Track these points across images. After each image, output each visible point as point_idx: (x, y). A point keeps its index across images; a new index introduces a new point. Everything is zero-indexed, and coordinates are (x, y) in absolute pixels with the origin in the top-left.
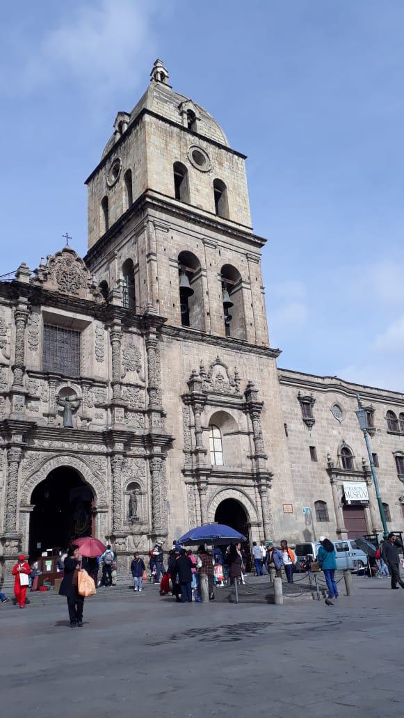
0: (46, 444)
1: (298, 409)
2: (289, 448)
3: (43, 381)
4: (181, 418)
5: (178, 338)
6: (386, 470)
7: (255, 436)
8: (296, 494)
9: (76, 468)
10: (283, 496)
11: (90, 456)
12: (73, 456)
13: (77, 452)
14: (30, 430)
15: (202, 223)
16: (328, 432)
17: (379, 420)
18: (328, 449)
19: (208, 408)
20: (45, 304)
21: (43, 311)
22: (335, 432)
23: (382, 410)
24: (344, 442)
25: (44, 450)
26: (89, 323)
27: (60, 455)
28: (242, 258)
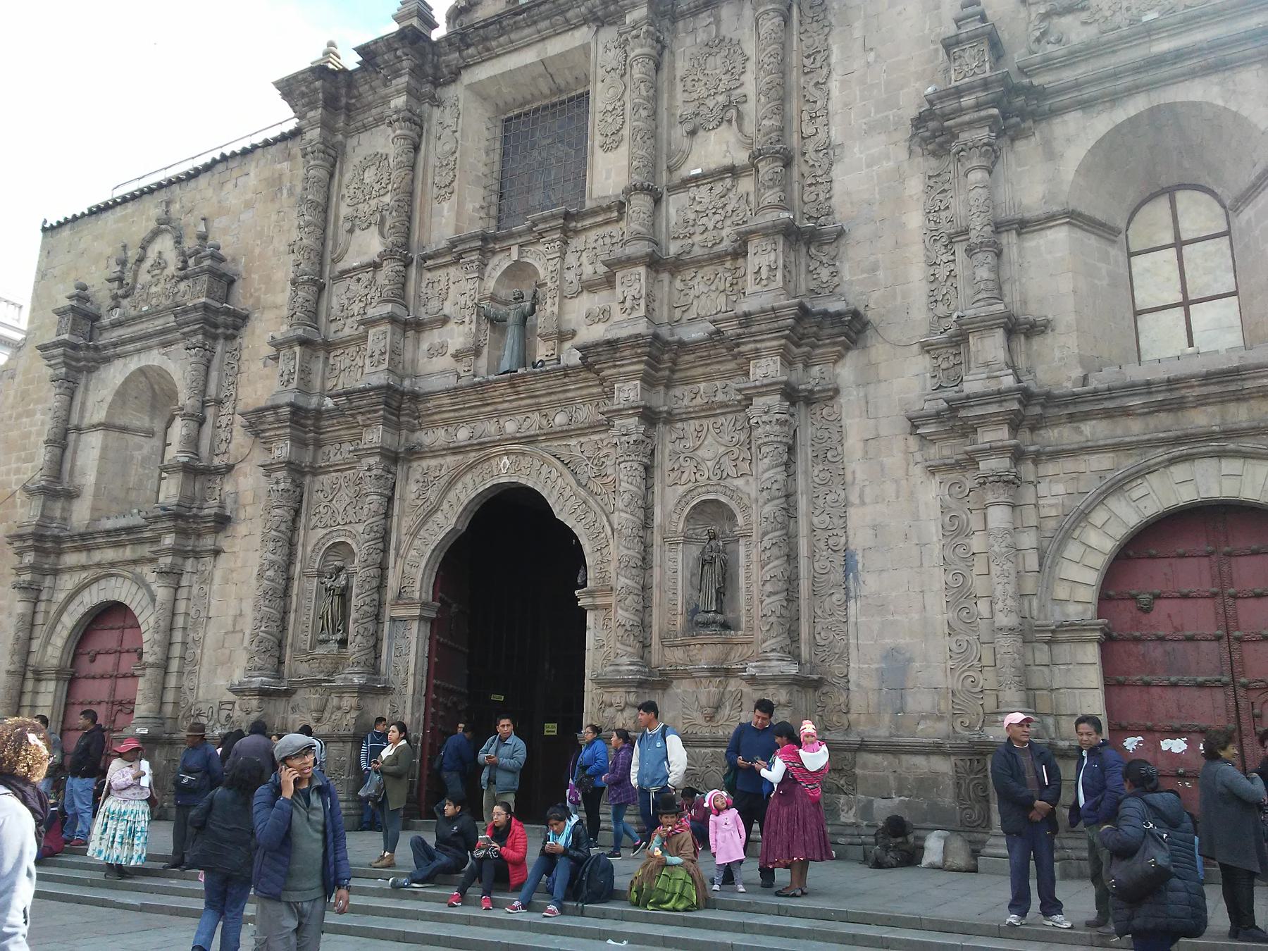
0: (463, 434)
3: (452, 271)
4: (915, 220)
9: (530, 484)
11: (573, 442)
12: (523, 454)
13: (531, 440)
19: (1069, 124)
20: (467, 66)
21: (470, 87)
25: (457, 450)
26: (585, 48)
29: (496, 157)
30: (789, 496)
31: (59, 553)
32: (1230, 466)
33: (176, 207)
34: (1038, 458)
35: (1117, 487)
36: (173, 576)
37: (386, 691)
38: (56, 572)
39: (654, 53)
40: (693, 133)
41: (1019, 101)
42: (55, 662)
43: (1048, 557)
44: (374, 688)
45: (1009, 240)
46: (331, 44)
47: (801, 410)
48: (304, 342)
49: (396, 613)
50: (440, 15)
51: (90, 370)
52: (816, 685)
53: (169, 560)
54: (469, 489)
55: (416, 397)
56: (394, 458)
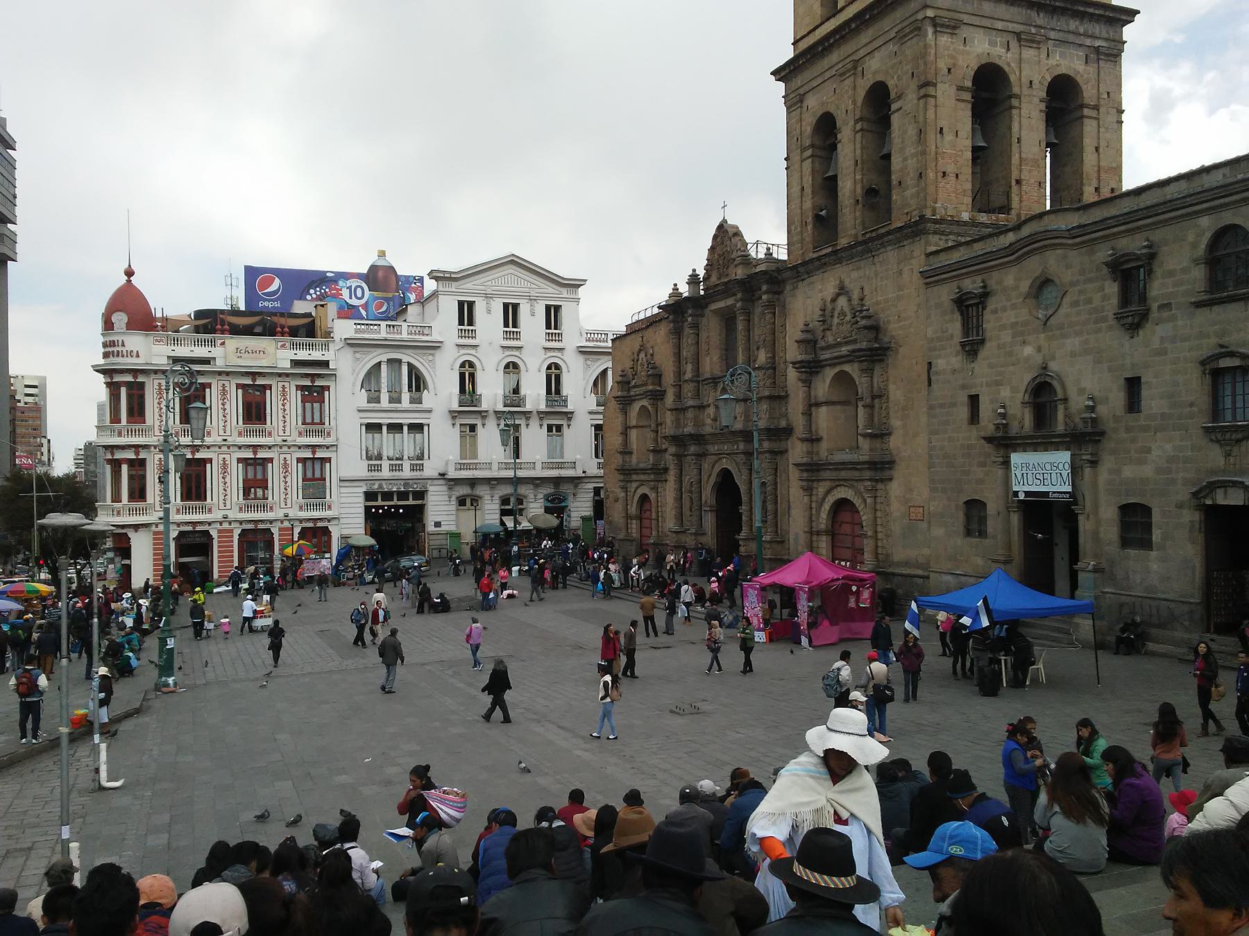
1: (955, 327)
2: (931, 408)
5: (802, 278)
6: (1163, 415)
7: (879, 396)
8: (933, 490)
10: (911, 490)
14: (698, 439)
15: (834, 42)
16: (1010, 354)
17: (1171, 273)
18: (1005, 393)
21: (712, 311)
22: (1028, 350)
23: (1191, 237)
24: (1045, 368)
25: (715, 454)
27: (721, 459)
28: (896, 49)
29: (724, 336)
30: (776, 483)
31: (631, 474)
32: (846, 489)
33: (645, 339)
34: (819, 481)
35: (828, 492)
36: (655, 489)
37: (704, 534)
38: (631, 481)
39: (747, 318)
40: (758, 349)
41: (812, 365)
42: (634, 513)
43: (819, 511)
44: (700, 533)
45: (813, 409)
46: (675, 285)
47: (778, 458)
48: (675, 410)
49: (706, 509)
50: (701, 277)
51: (630, 404)
52: (782, 542)
53: (652, 483)
54: (717, 469)
55: (703, 435)
56: (701, 456)
